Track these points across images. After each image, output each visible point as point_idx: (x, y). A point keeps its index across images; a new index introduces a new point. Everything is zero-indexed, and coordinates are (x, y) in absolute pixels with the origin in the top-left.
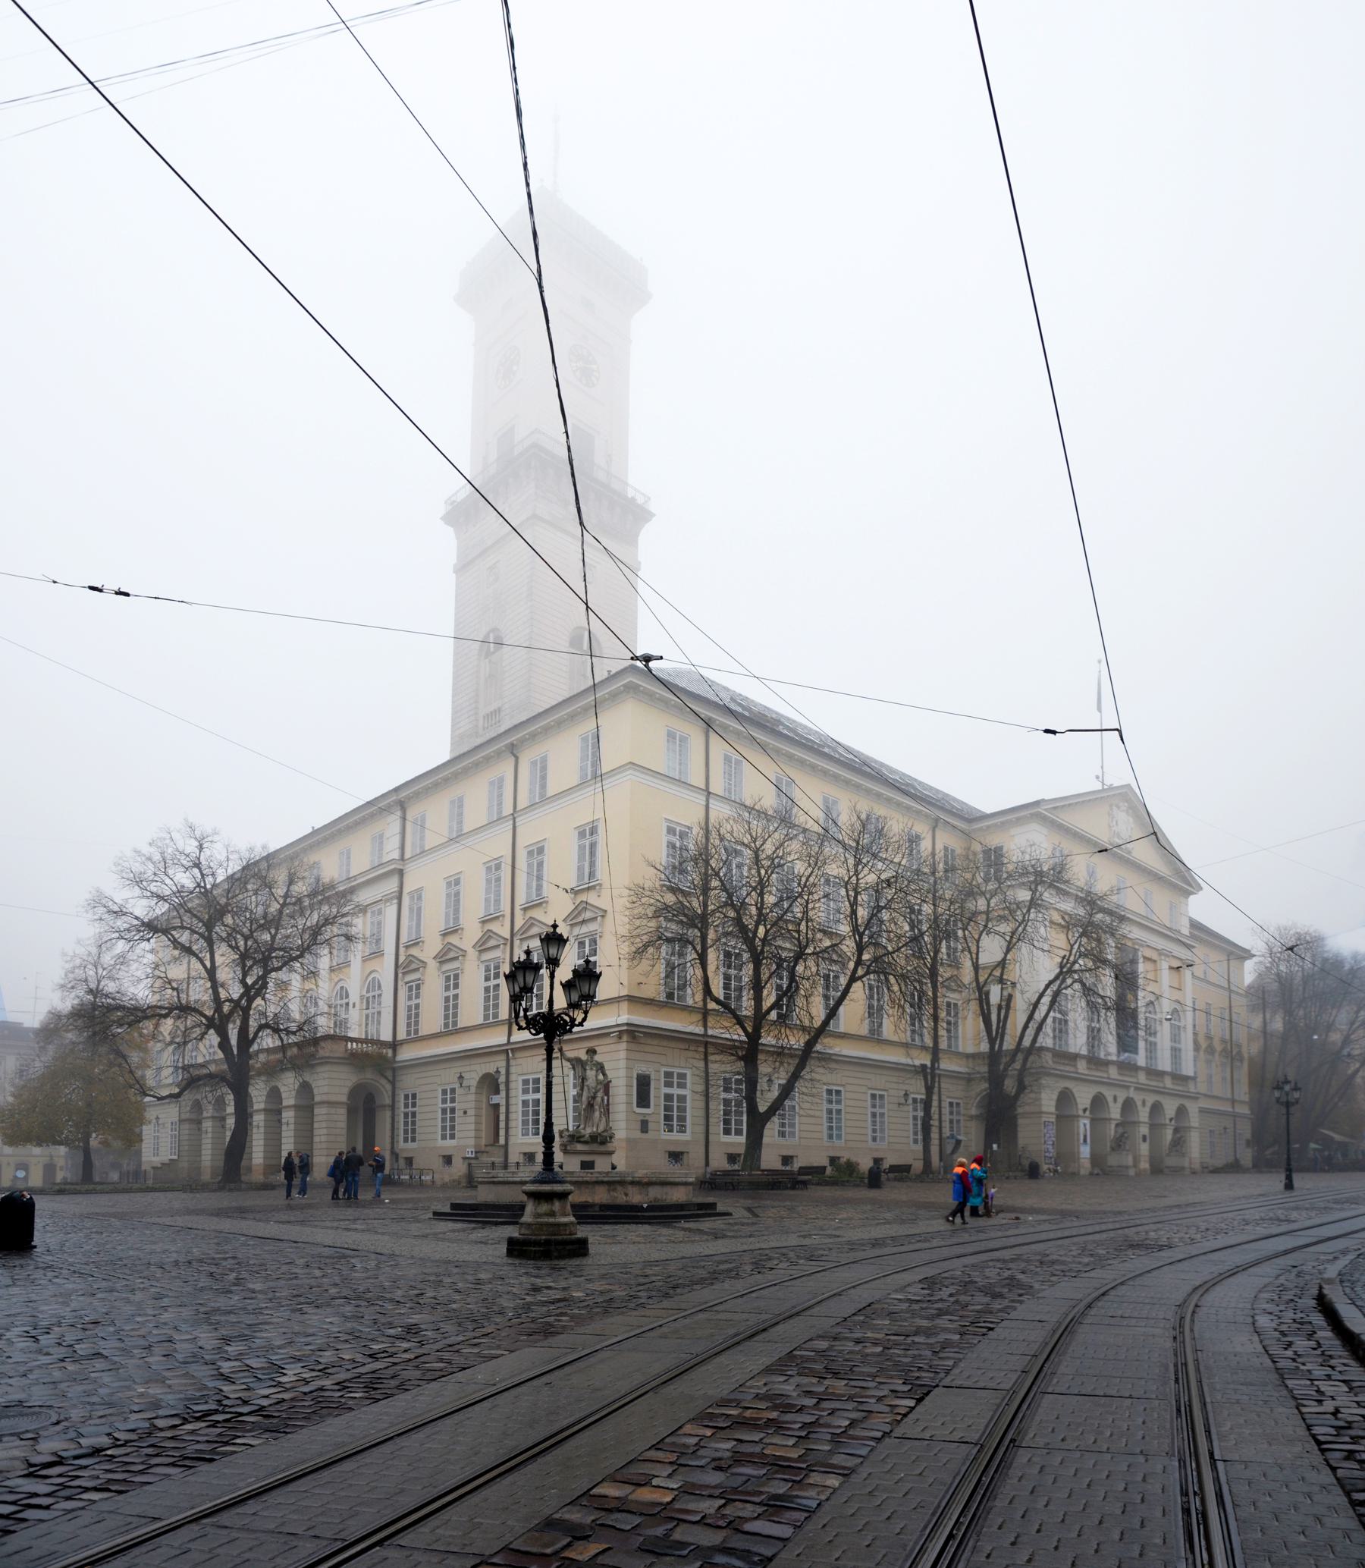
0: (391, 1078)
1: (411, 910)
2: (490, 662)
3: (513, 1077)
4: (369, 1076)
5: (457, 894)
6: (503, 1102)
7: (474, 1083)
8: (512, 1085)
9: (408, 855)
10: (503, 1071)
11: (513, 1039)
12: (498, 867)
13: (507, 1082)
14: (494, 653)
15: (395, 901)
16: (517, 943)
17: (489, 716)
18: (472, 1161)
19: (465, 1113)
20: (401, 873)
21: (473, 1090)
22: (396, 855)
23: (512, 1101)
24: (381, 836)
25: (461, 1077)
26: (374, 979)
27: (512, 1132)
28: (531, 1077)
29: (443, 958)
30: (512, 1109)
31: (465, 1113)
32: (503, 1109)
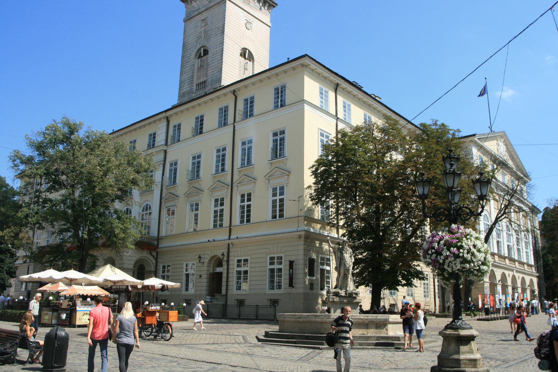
0: (155, 257)
1: (171, 170)
2: (201, 60)
3: (231, 258)
4: (145, 254)
5: (199, 163)
6: (225, 272)
7: (206, 261)
8: (231, 262)
9: (169, 143)
10: (226, 254)
11: (231, 237)
12: (224, 149)
13: (228, 261)
14: (203, 57)
15: (162, 165)
16: (235, 188)
17: (198, 85)
18: (209, 304)
19: (200, 276)
20: (165, 152)
21: (206, 264)
22: (163, 142)
23: (230, 271)
24: (155, 134)
25: (200, 257)
26: (147, 205)
27: (230, 288)
28: (242, 258)
29: (188, 195)
30: (230, 275)
31: (200, 276)
32: (224, 275)
